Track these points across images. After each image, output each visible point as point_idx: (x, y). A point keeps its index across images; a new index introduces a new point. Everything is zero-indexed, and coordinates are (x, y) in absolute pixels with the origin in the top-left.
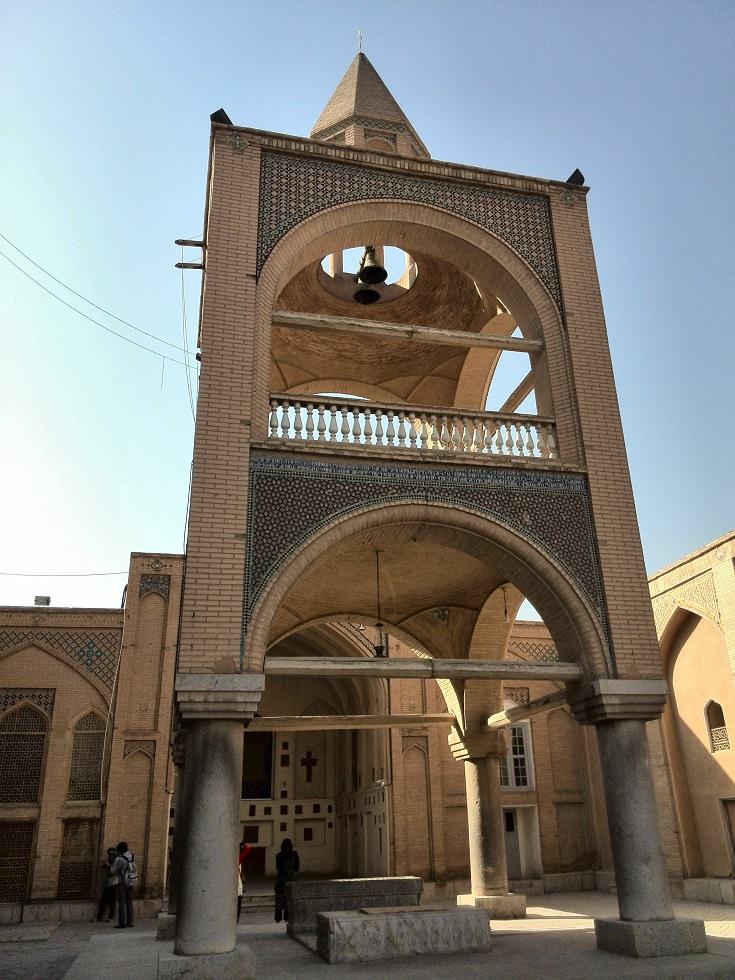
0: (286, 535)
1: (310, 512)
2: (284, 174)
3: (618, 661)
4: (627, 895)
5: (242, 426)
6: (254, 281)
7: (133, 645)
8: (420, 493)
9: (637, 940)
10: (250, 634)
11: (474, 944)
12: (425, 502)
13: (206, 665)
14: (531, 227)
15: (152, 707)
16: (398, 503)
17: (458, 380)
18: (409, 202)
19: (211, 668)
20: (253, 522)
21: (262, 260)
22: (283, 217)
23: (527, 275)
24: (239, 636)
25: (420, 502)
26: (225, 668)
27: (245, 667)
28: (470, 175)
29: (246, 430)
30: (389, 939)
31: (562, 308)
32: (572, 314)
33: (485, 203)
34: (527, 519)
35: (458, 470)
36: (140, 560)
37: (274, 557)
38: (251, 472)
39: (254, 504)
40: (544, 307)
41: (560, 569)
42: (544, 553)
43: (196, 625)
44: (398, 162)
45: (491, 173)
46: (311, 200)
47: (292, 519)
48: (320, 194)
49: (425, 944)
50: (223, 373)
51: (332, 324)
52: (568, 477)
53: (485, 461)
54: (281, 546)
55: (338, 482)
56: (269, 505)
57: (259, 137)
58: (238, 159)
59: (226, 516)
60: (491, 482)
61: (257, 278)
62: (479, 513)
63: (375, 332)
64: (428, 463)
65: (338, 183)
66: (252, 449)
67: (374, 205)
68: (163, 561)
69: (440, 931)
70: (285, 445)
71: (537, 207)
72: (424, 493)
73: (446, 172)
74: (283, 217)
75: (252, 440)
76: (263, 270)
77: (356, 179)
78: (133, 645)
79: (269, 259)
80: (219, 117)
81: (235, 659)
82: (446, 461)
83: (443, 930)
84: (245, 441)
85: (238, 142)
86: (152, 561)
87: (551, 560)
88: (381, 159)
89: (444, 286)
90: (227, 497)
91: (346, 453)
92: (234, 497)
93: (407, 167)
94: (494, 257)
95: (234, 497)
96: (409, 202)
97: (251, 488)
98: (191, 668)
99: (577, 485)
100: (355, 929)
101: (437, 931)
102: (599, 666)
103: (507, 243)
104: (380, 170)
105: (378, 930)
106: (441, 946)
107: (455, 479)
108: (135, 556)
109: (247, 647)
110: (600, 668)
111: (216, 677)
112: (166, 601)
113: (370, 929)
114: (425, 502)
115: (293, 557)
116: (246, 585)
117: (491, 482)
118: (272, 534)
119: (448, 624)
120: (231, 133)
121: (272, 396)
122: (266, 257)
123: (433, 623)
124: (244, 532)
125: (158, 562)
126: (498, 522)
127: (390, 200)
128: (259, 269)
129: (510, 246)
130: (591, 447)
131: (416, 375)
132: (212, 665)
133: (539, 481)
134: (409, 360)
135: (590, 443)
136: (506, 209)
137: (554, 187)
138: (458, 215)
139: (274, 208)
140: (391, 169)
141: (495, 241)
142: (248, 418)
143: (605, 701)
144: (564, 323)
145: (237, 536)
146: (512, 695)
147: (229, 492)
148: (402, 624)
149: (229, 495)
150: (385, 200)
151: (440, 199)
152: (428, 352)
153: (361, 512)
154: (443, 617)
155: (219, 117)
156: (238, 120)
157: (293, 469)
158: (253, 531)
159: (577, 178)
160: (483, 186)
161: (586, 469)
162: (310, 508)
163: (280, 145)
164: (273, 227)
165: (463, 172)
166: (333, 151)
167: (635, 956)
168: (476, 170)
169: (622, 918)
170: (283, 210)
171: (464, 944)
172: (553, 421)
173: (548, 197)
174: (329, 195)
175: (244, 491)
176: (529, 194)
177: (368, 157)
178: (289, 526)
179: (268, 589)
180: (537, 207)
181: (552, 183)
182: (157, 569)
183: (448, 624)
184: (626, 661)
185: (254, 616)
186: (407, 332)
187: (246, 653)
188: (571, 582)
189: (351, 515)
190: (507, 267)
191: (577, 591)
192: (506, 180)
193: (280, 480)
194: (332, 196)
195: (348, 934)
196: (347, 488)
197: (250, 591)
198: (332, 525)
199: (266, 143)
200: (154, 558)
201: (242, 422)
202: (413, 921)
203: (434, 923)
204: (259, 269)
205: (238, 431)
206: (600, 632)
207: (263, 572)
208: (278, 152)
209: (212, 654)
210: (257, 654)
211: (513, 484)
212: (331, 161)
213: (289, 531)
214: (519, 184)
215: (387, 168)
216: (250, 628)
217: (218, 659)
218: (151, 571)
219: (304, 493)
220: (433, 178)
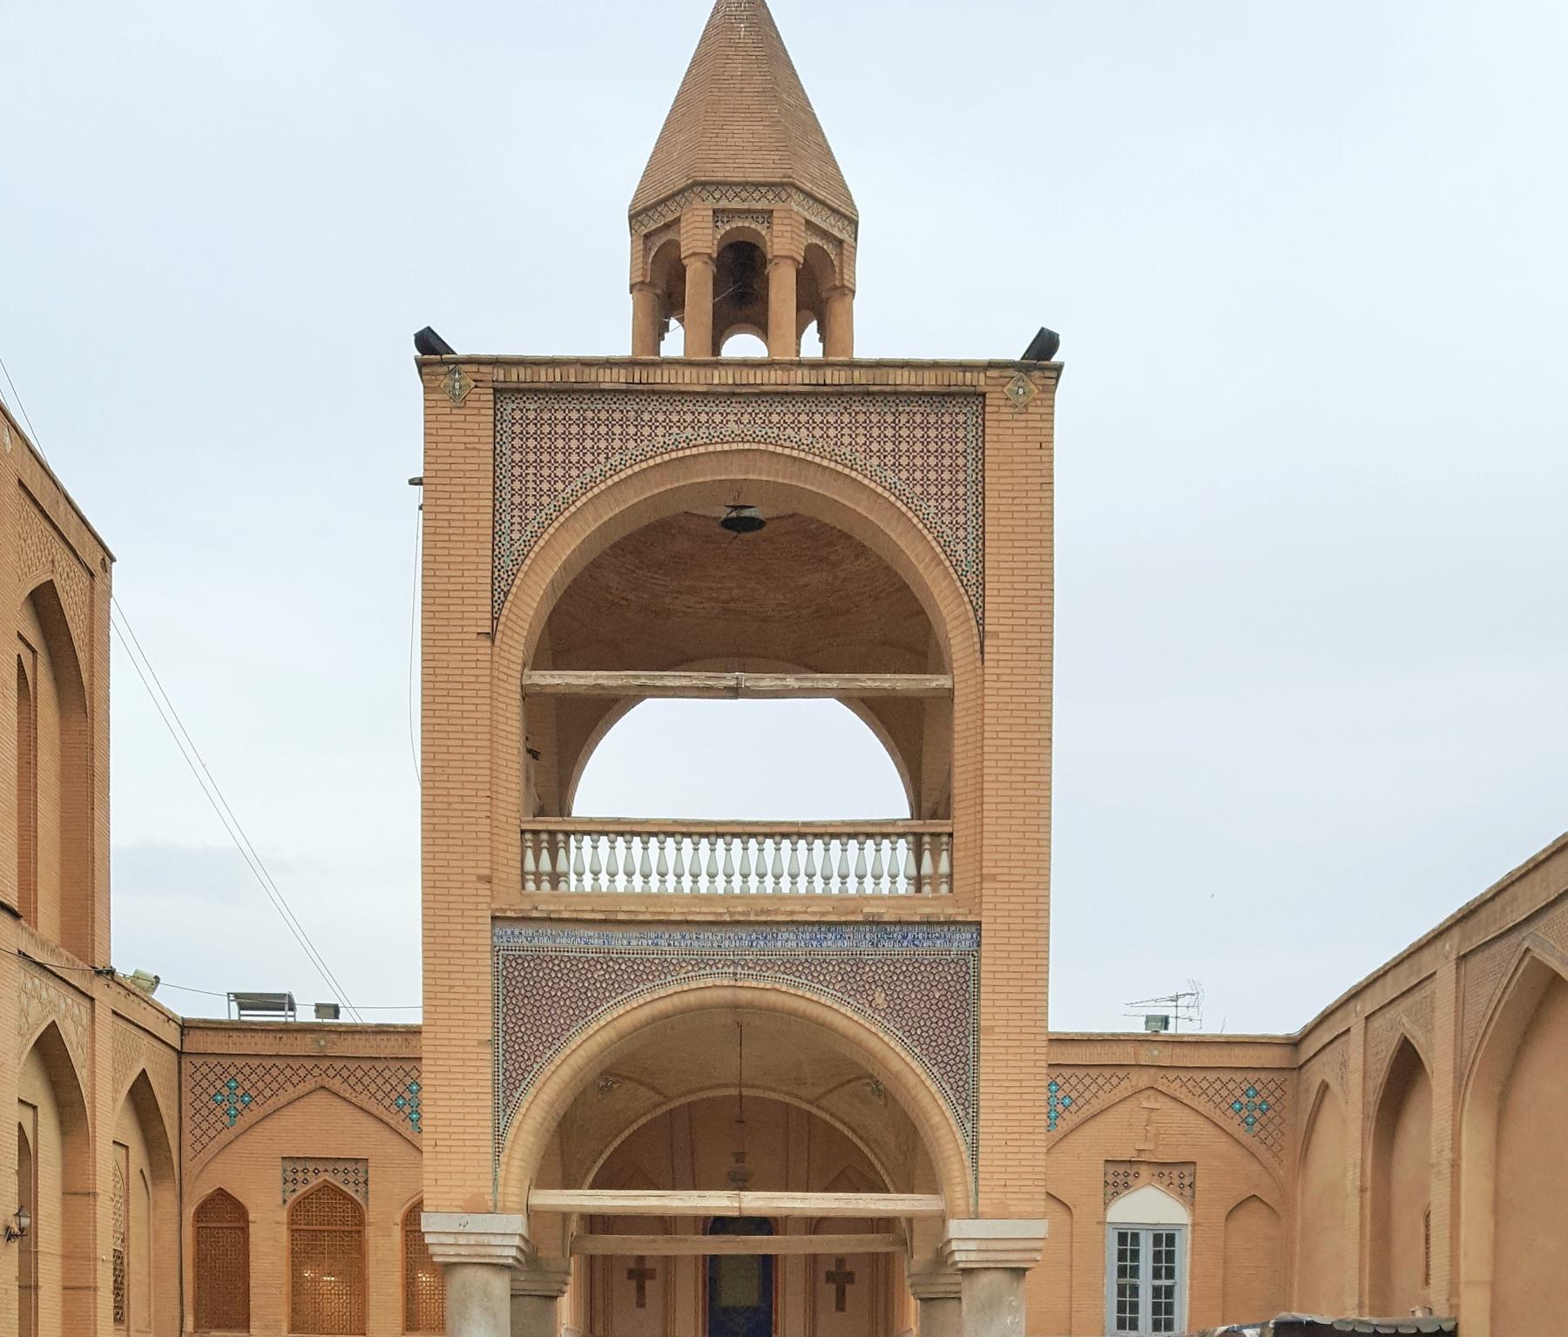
2: (532, 428)
5: (479, 885)
6: (488, 643)
8: (725, 969)
10: (503, 1167)
12: (732, 983)
14: (947, 462)
16: (693, 985)
18: (734, 446)
20: (501, 1022)
22: (531, 514)
24: (490, 1170)
25: (726, 983)
26: (475, 1207)
27: (500, 1205)
29: (484, 889)
31: (981, 623)
32: (996, 635)
33: (867, 425)
34: (880, 999)
35: (784, 929)
37: (529, 1069)
38: (495, 951)
39: (501, 997)
41: (919, 1071)
42: (898, 1049)
43: (439, 1156)
44: (716, 373)
47: (551, 1015)
48: (589, 458)
52: (953, 928)
53: (823, 914)
55: (611, 959)
56: (520, 998)
60: (831, 944)
61: (491, 636)
62: (808, 995)
64: (739, 922)
66: (494, 918)
71: (961, 418)
72: (731, 970)
75: (493, 906)
76: (502, 619)
77: (646, 417)
79: (510, 597)
80: (428, 343)
81: (487, 1197)
82: (763, 918)
84: (485, 906)
87: (909, 1059)
88: (687, 372)
91: (621, 917)
95: (475, 990)
97: (496, 974)
102: (959, 1202)
107: (779, 944)
109: (501, 1181)
110: (960, 1204)
115: (553, 1067)
116: (496, 1106)
120: (445, 369)
121: (525, 827)
122: (506, 595)
126: (836, 1006)
130: (993, 878)
132: (461, 1203)
136: (905, 432)
140: (704, 389)
142: (487, 872)
143: (954, 1246)
145: (481, 1043)
147: (467, 983)
151: (789, 431)
153: (641, 1001)
155: (428, 343)
157: (550, 943)
158: (501, 1034)
159: (1045, 344)
161: (980, 914)
162: (574, 999)
164: (516, 536)
170: (531, 501)
172: (949, 829)
175: (486, 981)
176: (949, 394)
177: (666, 373)
178: (546, 1026)
180: (961, 418)
184: (994, 1196)
185: (508, 1144)
187: (500, 1189)
188: (934, 1088)
192: (906, 372)
194: (607, 458)
196: (623, 967)
197: (501, 1114)
199: (501, 378)
201: (480, 878)
204: (495, 619)
206: (965, 1157)
207: (516, 1088)
208: (519, 391)
209: (460, 1190)
210: (514, 1191)
211: (865, 946)
213: (547, 1032)
214: (929, 380)
216: (503, 1158)
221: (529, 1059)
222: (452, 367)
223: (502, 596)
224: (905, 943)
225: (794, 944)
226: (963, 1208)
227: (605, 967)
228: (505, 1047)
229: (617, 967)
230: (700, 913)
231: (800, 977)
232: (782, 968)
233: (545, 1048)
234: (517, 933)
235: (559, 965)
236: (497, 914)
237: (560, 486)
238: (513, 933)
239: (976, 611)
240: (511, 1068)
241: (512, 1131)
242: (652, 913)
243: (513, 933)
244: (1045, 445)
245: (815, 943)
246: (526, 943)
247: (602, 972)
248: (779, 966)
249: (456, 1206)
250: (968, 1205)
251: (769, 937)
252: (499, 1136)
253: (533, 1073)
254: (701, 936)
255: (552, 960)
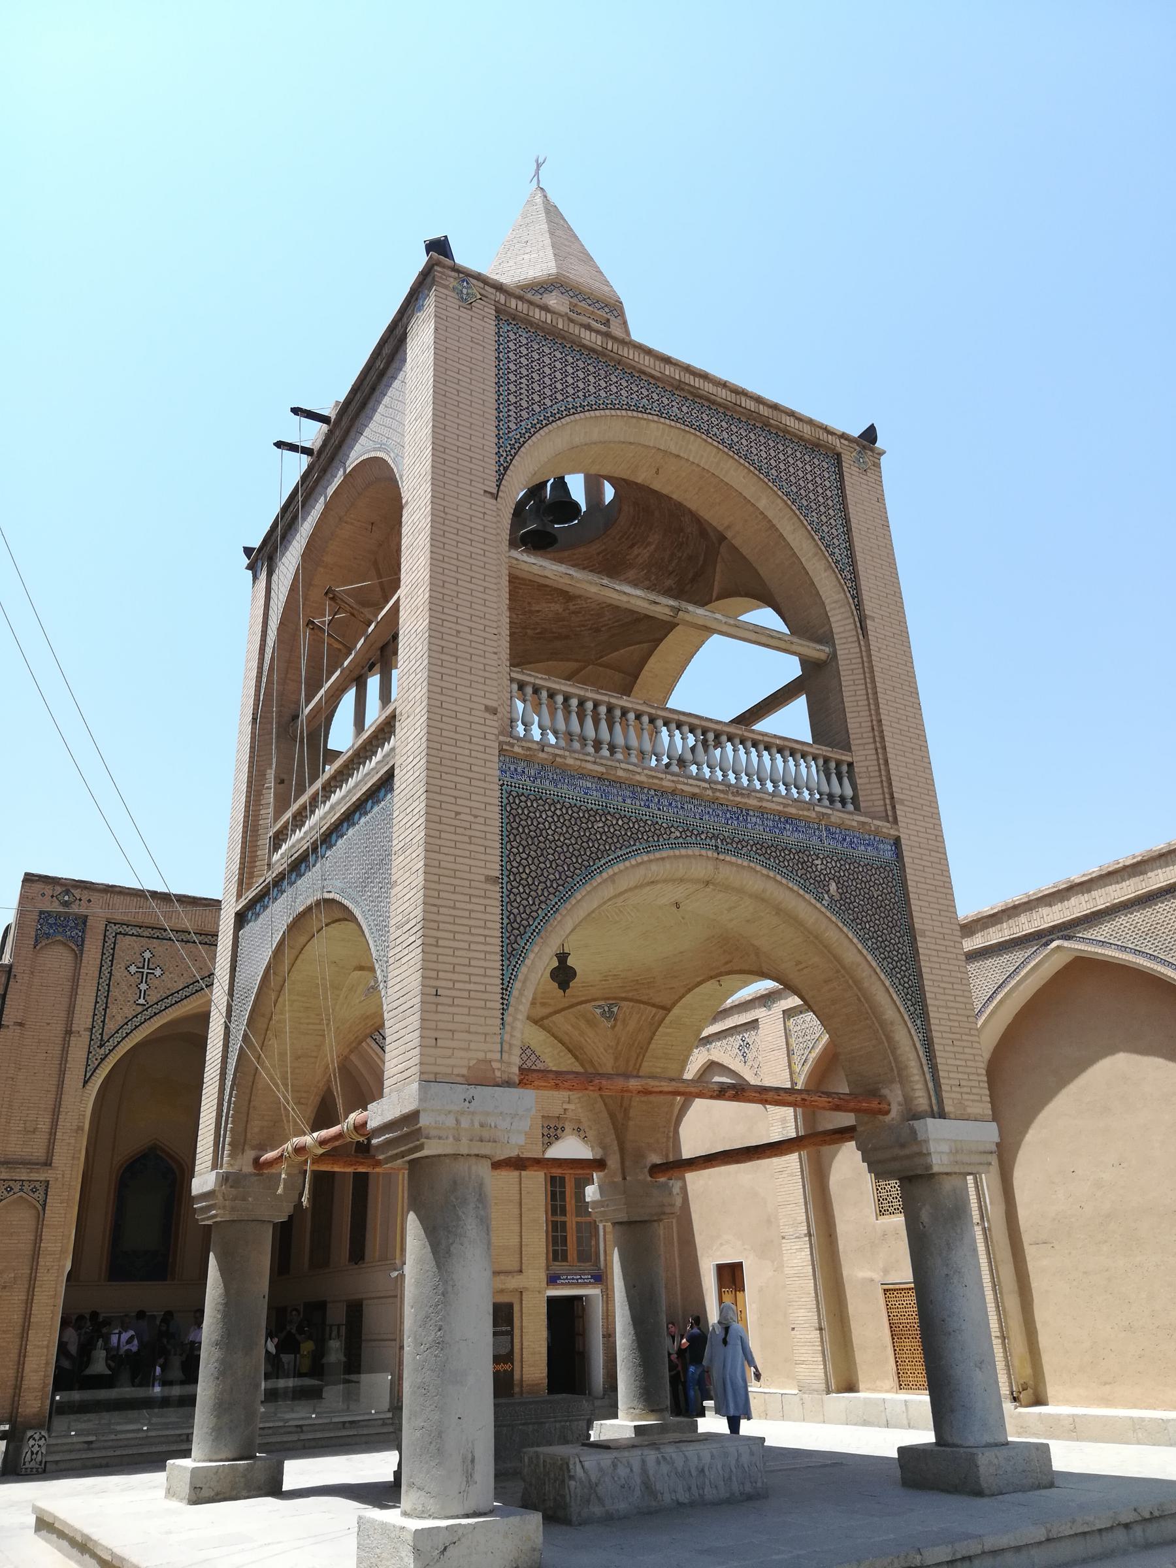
0: (548, 884)
1: (576, 853)
3: (944, 1095)
4: (952, 1411)
5: (487, 715)
7: (21, 1024)
9: (982, 1470)
11: (748, 1488)
13: (456, 1071)
15: (44, 1125)
17: (637, 677)
19: (463, 1076)
21: (502, 471)
22: (524, 414)
23: (816, 554)
28: (751, 405)
30: (647, 1486)
31: (859, 606)
33: (766, 445)
36: (38, 887)
37: (534, 914)
40: (836, 602)
43: (440, 1008)
45: (775, 407)
46: (560, 397)
49: (690, 1489)
50: (458, 632)
51: (578, 581)
54: (542, 898)
55: (609, 813)
57: (493, 291)
58: (465, 314)
59: (472, 847)
61: (495, 497)
63: (633, 601)
65: (592, 380)
67: (634, 420)
68: (77, 893)
69: (706, 1470)
70: (543, 751)
73: (723, 393)
74: (524, 414)
75: (502, 738)
78: (21, 1024)
79: (508, 472)
80: (439, 247)
81: (495, 1065)
83: (710, 1468)
84: (493, 737)
85: (465, 291)
86: (59, 889)
88: (647, 358)
89: (649, 544)
90: (472, 819)
92: (482, 820)
93: (677, 377)
94: (775, 522)
96: (678, 425)
98: (436, 1074)
99: (888, 853)
100: (601, 1470)
101: (703, 1471)
103: (793, 507)
104: (644, 373)
105: (632, 1470)
106: (710, 1494)
107: (749, 826)
108: (29, 879)
111: (473, 1091)
112: (78, 957)
113: (622, 1471)
114: (715, 855)
117: (791, 837)
118: (530, 880)
119: (613, 1027)
123: (592, 1023)
124: (498, 874)
125: (67, 892)
127: (656, 418)
128: (499, 482)
129: (798, 512)
131: (577, 661)
132: (464, 1071)
133: (844, 840)
134: (567, 637)
135: (901, 797)
137: (846, 443)
138: (736, 457)
139: (512, 399)
140: (659, 375)
141: (779, 501)
142: (493, 704)
144: (864, 629)
145: (489, 879)
146: (579, 1130)
147: (474, 812)
148: (546, 1022)
149: (476, 817)
150: (650, 417)
151: (714, 429)
152: (598, 630)
154: (609, 1015)
155: (439, 247)
156: (463, 256)
160: (766, 424)
163: (520, 308)
164: (513, 427)
165: (743, 399)
166: (588, 332)
167: (979, 1493)
168: (759, 400)
169: (938, 1443)
170: (525, 405)
171: (735, 1487)
172: (850, 759)
173: (839, 455)
174: (580, 394)
175: (494, 813)
177: (631, 352)
179: (528, 962)
181: (843, 436)
182: (66, 904)
183: (613, 1027)
186: (672, 607)
189: (627, 863)
190: (790, 538)
191: (895, 996)
193: (536, 800)
195: (594, 1479)
197: (506, 963)
198: (605, 875)
199: (503, 301)
200: (62, 885)
201: (488, 709)
202: (674, 1455)
203: (699, 1458)
204: (499, 482)
205: (482, 721)
207: (521, 935)
209: (462, 1054)
212: (584, 346)
214: (807, 430)
215: (653, 372)
217: (472, 1063)
218: (56, 907)
219: (567, 823)
220: (708, 400)
221: (534, 903)
222: (461, 275)
223: (502, 468)
224: (845, 845)
225: (761, 828)
226: (926, 1108)
227: (603, 819)
228: (509, 887)
229: (614, 822)
230: (687, 784)
231: (769, 859)
232: (754, 849)
233: (550, 894)
234: (519, 770)
235: (561, 809)
236: (504, 747)
237: (547, 402)
238: (516, 770)
239: (853, 599)
240: (515, 911)
241: (518, 985)
242: (647, 775)
243: (516, 770)
244: (881, 500)
245: (777, 831)
246: (528, 782)
247: (601, 825)
248: (752, 846)
249: (458, 1075)
250: (931, 1106)
251: (741, 818)
252: (506, 990)
253: (538, 920)
254: (685, 807)
255: (554, 803)
